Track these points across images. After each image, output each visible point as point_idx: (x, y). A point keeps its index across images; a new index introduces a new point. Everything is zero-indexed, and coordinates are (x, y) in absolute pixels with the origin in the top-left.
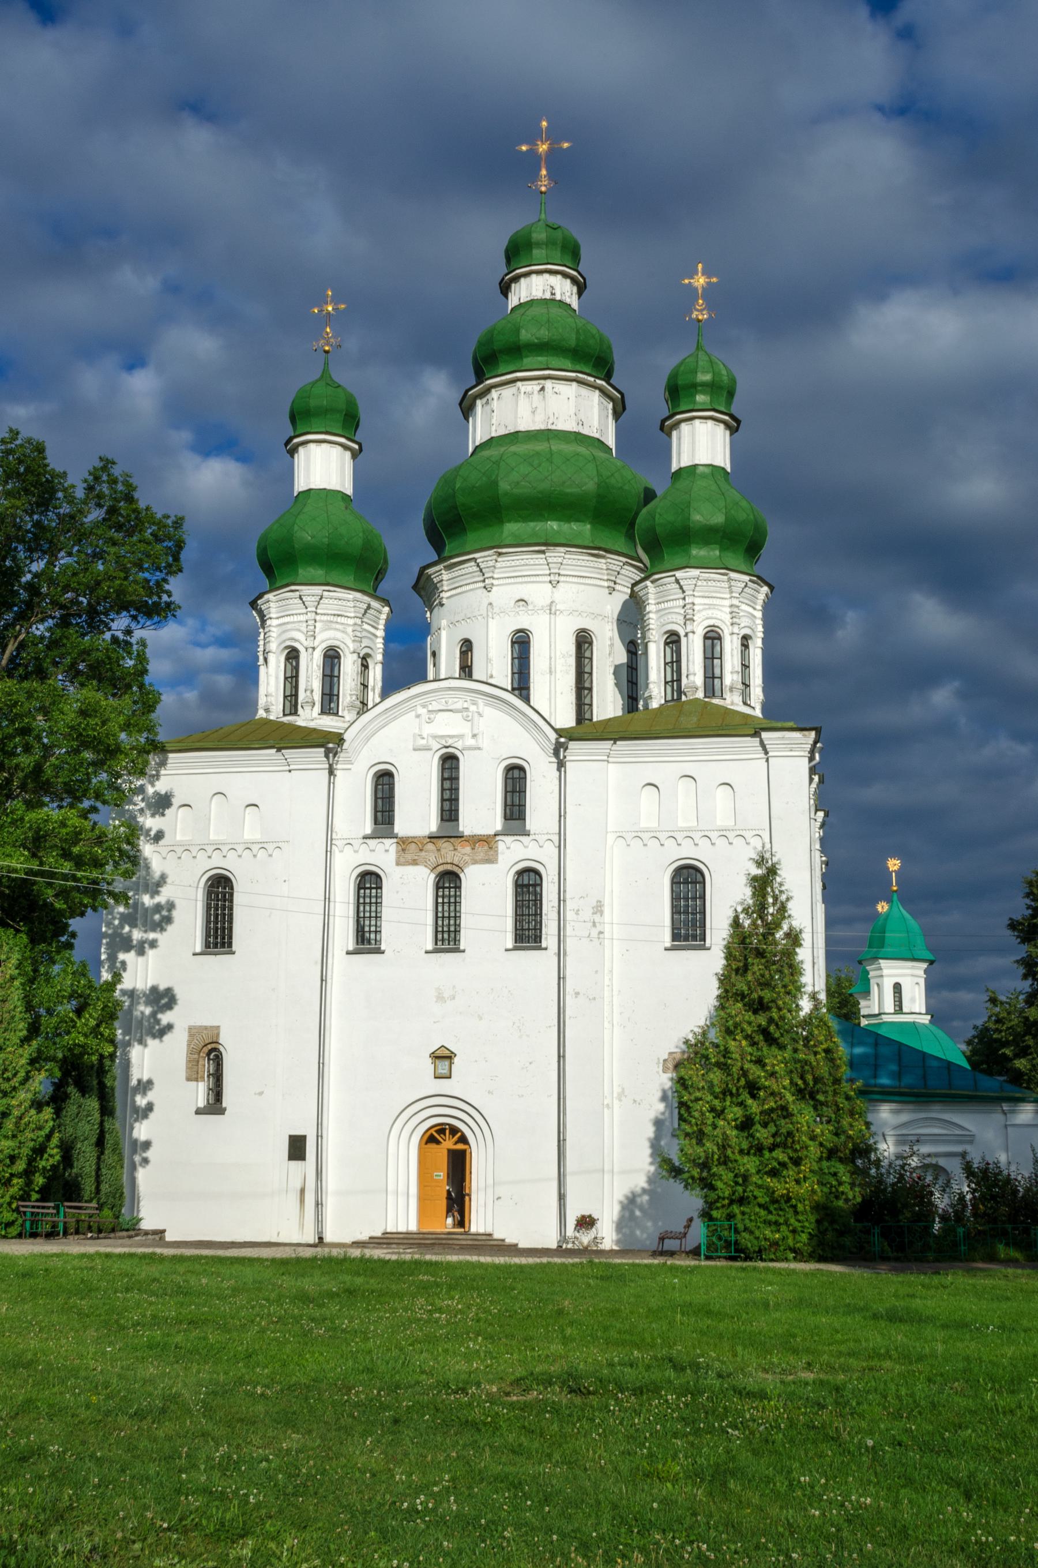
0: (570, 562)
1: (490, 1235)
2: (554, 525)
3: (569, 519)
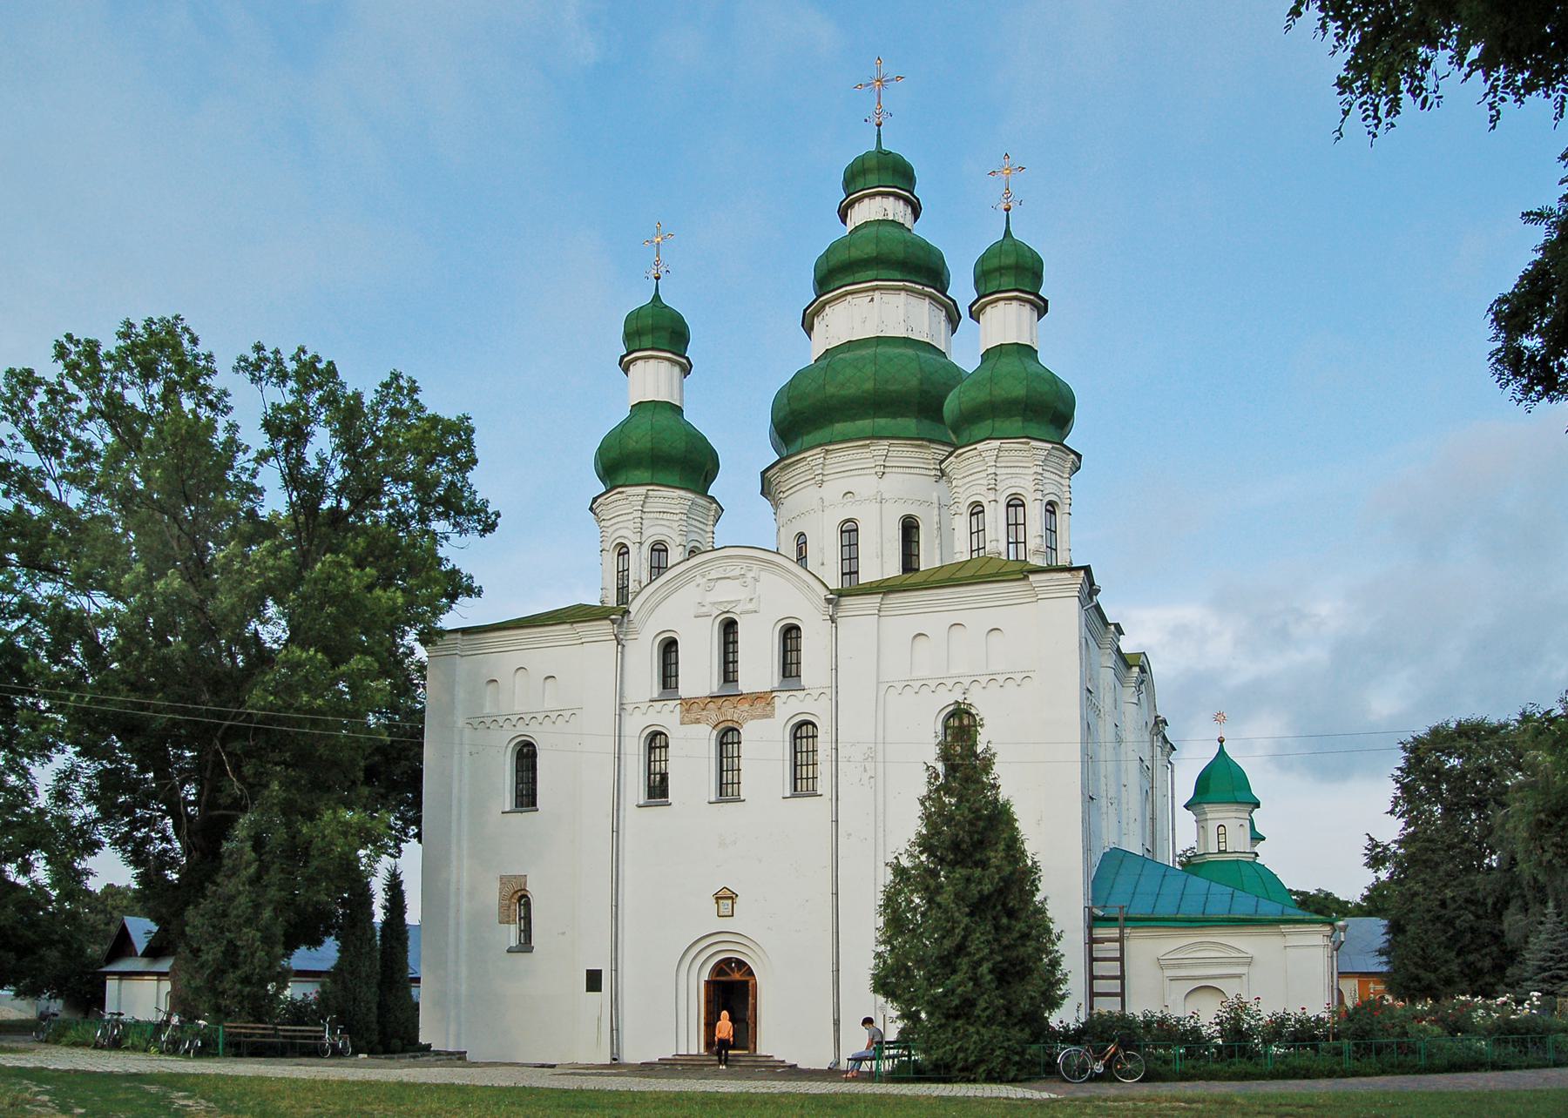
0: (894, 454)
2: (882, 421)
3: (894, 416)
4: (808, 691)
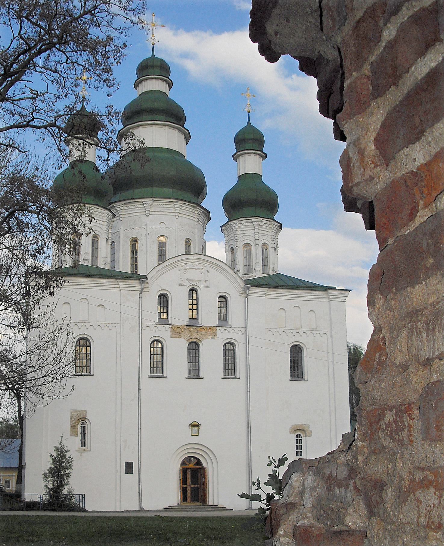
4: (233, 329)
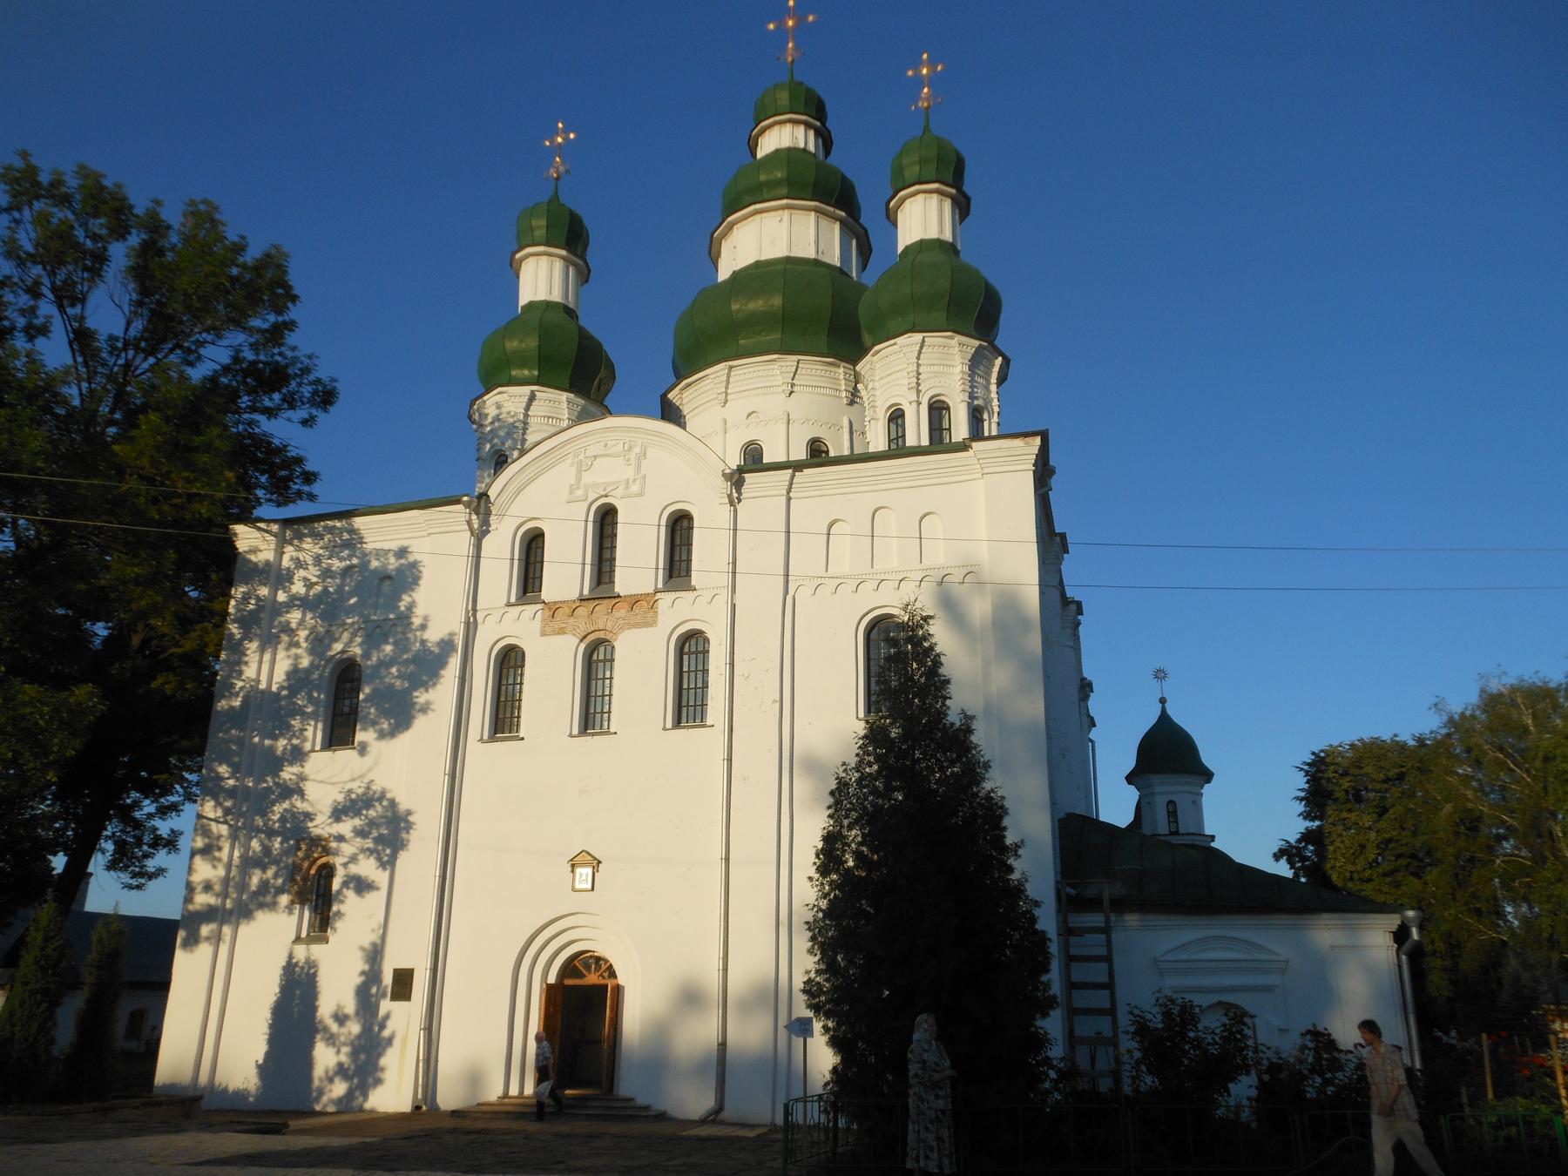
1: (632, 1099)
